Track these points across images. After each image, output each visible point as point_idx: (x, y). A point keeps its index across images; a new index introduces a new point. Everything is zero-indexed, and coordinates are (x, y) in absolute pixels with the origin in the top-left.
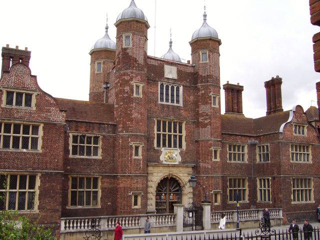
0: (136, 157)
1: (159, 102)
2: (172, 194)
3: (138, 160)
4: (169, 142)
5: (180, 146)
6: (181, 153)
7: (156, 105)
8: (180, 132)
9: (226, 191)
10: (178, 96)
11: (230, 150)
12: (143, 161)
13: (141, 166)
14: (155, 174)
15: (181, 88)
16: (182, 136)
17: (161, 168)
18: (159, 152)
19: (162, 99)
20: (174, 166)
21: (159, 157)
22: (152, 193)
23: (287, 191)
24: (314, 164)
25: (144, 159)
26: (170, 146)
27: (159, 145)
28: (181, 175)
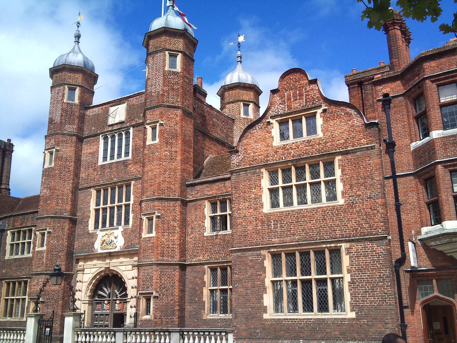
0: (41, 249)
1: (101, 162)
2: (118, 302)
3: (41, 252)
4: (105, 220)
5: (127, 222)
6: (125, 233)
7: (94, 170)
8: (128, 199)
9: (202, 293)
10: (127, 145)
11: (214, 210)
12: (47, 254)
13: (44, 260)
14: (86, 271)
15: (131, 130)
16: (129, 205)
17: (95, 262)
18: (93, 236)
19: (105, 158)
20: (111, 255)
21: (93, 244)
22: (79, 300)
23: (249, 284)
24: (350, 205)
25: (48, 251)
26: (111, 224)
27: (96, 227)
28: (123, 268)
